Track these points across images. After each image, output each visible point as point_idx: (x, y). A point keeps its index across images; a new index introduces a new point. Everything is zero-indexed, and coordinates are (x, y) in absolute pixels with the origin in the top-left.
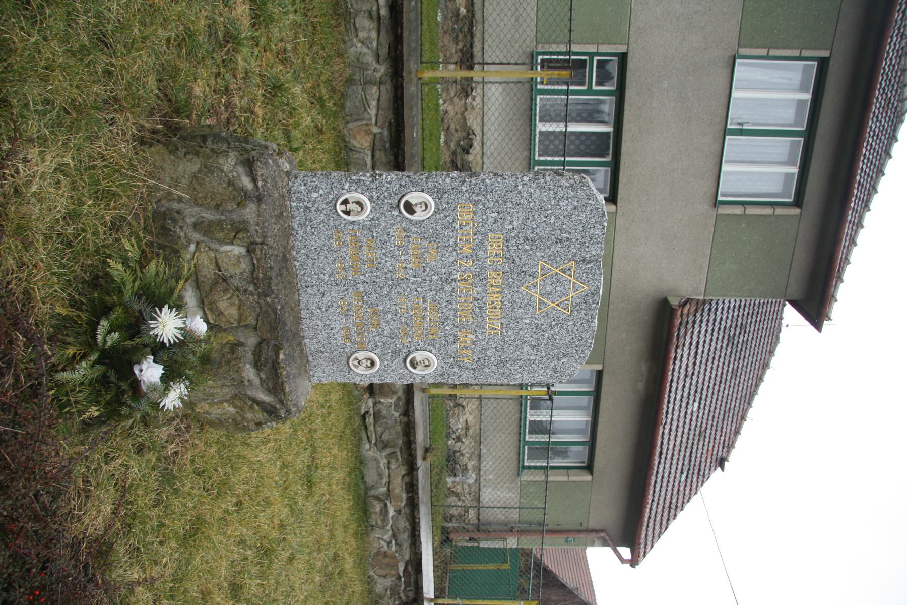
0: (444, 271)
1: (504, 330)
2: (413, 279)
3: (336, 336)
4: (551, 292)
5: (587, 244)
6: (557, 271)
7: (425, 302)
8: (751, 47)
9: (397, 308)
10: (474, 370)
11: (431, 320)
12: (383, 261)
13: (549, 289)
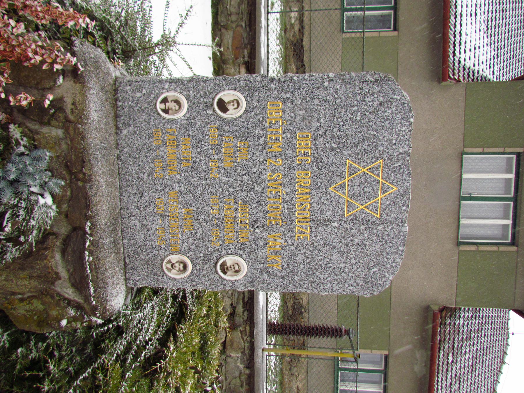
0: (254, 170)
1: (313, 235)
2: (225, 178)
3: (152, 237)
4: (359, 193)
5: (394, 142)
6: (365, 170)
7: (236, 203)
8: (471, 147)
9: (210, 208)
10: (283, 278)
11: (241, 222)
12: (198, 160)
13: (357, 189)
